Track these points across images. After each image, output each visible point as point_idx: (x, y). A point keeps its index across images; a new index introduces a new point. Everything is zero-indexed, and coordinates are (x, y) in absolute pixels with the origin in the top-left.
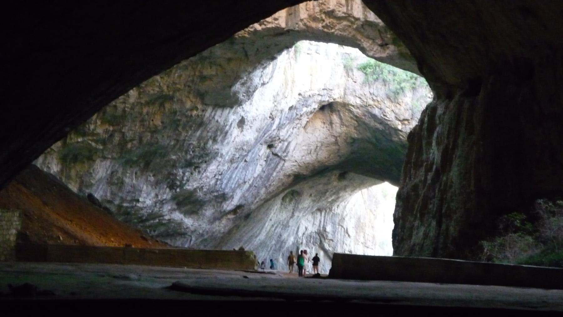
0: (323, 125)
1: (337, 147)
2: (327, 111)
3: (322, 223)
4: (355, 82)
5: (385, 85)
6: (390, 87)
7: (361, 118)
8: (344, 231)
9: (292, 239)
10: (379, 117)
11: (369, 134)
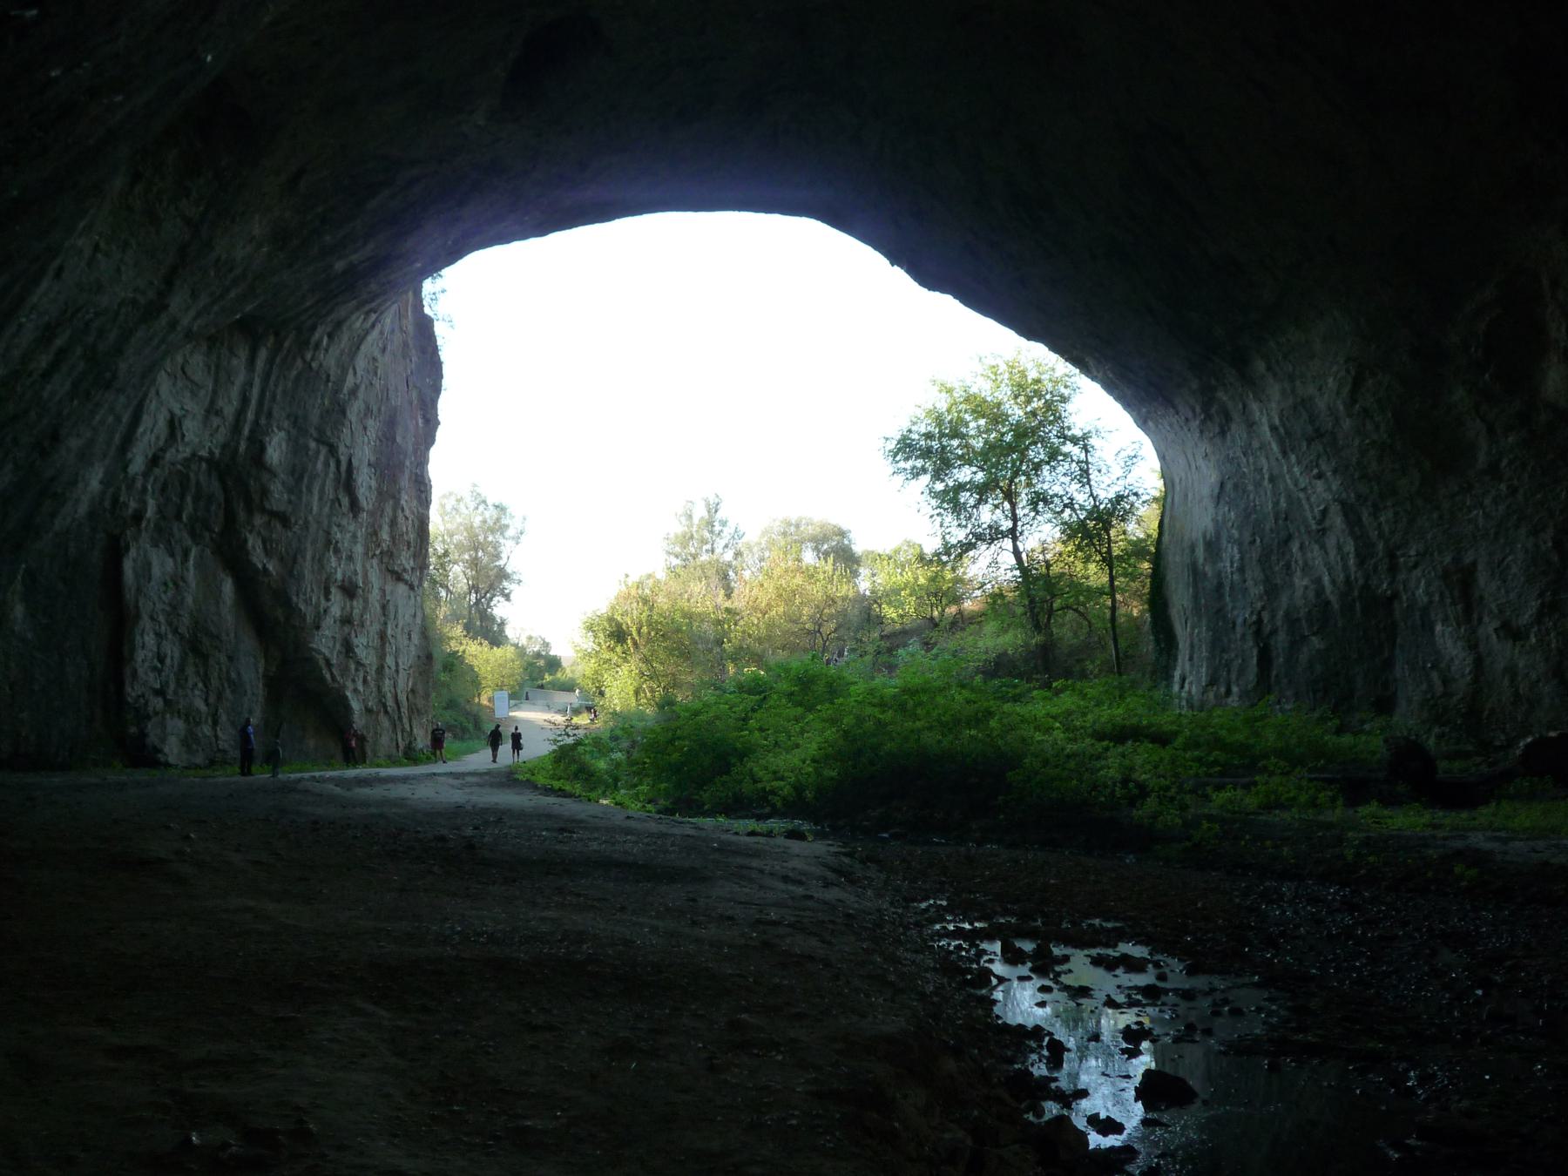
3: (250, 416)
8: (337, 480)
9: (94, 480)
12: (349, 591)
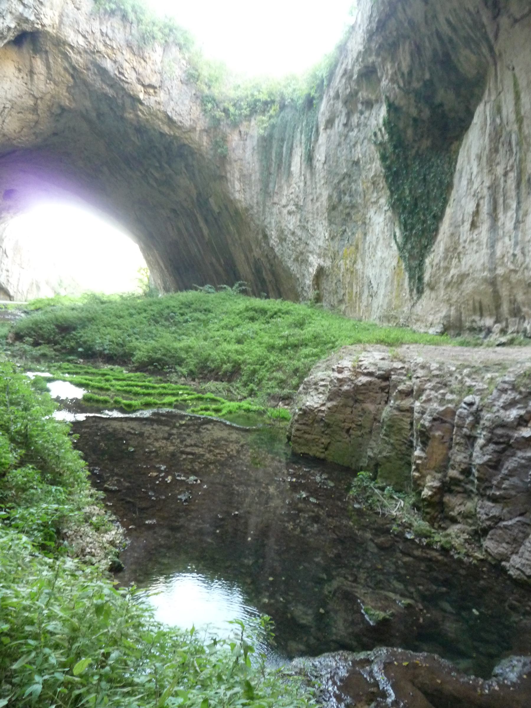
0: (17, 74)
1: (35, 117)
2: (27, 48)
4: (78, 9)
5: (125, 27)
6: (133, 32)
7: (82, 73)
10: (112, 74)
11: (88, 103)
12: (8, 271)
